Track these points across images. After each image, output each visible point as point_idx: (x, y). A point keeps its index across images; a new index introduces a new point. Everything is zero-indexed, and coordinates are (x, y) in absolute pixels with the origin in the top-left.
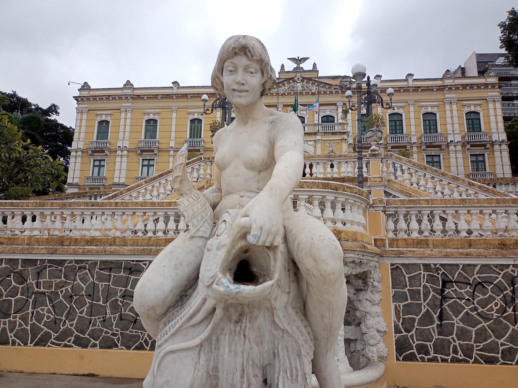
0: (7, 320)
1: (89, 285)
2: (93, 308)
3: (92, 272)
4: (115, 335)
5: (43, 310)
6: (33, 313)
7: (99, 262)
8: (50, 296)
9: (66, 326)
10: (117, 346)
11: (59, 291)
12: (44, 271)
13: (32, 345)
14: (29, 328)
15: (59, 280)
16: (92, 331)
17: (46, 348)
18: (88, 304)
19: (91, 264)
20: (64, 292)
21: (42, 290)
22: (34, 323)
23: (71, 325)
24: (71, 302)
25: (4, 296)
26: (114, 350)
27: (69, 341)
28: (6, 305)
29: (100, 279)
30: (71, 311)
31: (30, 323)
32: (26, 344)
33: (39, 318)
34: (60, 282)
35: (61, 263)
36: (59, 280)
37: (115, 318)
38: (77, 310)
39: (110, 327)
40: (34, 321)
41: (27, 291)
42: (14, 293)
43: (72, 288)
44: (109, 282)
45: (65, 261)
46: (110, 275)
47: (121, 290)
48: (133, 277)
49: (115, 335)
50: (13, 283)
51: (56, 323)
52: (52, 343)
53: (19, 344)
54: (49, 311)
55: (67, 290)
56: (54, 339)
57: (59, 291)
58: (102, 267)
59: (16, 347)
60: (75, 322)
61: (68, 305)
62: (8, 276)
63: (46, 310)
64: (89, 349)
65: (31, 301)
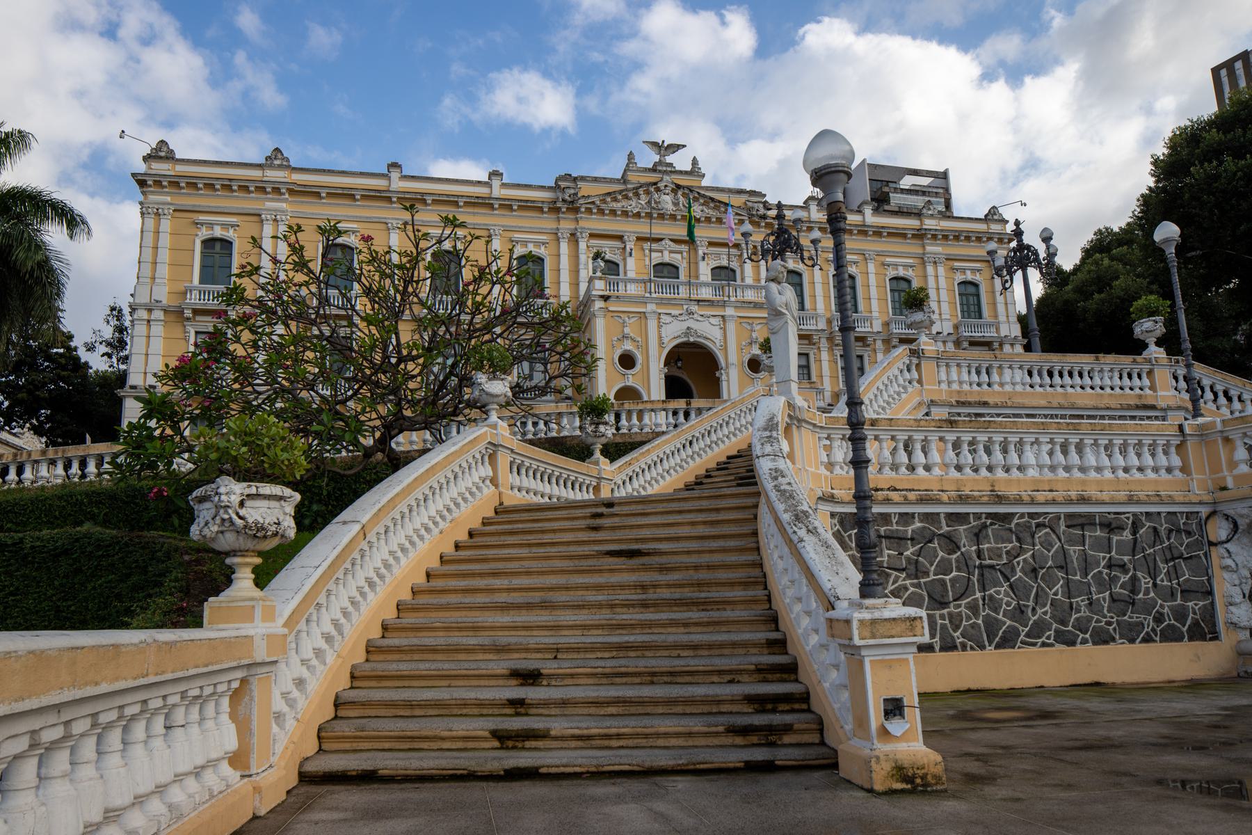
0: (945, 611)
1: (1056, 552)
4: (1109, 623)
5: (998, 593)
6: (984, 600)
10: (1113, 640)
13: (992, 647)
14: (980, 622)
16: (1077, 619)
17: (1016, 650)
21: (988, 562)
23: (1045, 612)
26: (1112, 646)
27: (1048, 638)
28: (939, 588)
29: (1072, 542)
32: (982, 647)
33: (994, 604)
34: (1013, 548)
35: (1007, 517)
37: (1104, 599)
39: (1099, 612)
41: (965, 563)
42: (944, 568)
45: (1013, 515)
46: (1083, 535)
47: (1104, 558)
48: (1115, 538)
49: (1109, 623)
51: (1022, 612)
54: (1007, 595)
58: (1069, 523)
60: (1048, 608)
62: (930, 541)
63: (1001, 591)
64: (1078, 646)
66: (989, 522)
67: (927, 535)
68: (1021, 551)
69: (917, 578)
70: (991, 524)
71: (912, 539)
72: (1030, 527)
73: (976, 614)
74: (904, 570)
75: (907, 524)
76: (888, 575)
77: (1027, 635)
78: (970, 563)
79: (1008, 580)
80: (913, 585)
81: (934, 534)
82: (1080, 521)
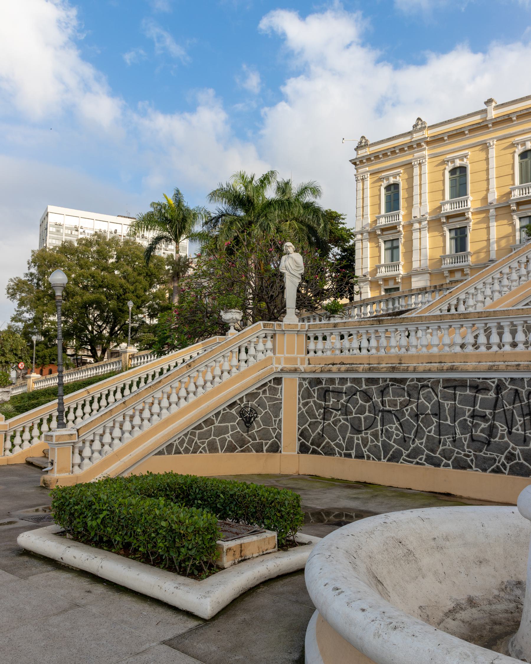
0: (359, 436)
1: (434, 404)
2: (441, 427)
3: (436, 391)
6: (382, 430)
7: (441, 380)
8: (396, 414)
9: (415, 444)
11: (404, 409)
12: (387, 390)
13: (385, 460)
14: (380, 444)
15: (403, 399)
17: (399, 464)
18: (435, 424)
19: (433, 382)
20: (409, 410)
21: (388, 408)
22: (384, 440)
24: (418, 421)
25: (354, 413)
29: (445, 398)
30: (419, 430)
31: (381, 439)
32: (379, 459)
34: (404, 401)
36: (403, 399)
38: (425, 429)
40: (384, 438)
41: (374, 408)
42: (361, 411)
43: (417, 407)
44: (455, 401)
46: (455, 394)
50: (360, 402)
51: (405, 441)
52: (404, 460)
53: (373, 459)
55: (412, 408)
56: (406, 456)
57: (404, 409)
58: (446, 385)
59: (371, 461)
61: (415, 424)
62: (355, 394)
63: (394, 427)
65: (379, 418)
66: (390, 383)
67: (354, 391)
68: (409, 403)
69: (346, 415)
70: (392, 385)
71: (345, 393)
72: (417, 387)
73: (378, 440)
74: (340, 410)
75: (343, 384)
76: (332, 413)
77: (408, 456)
78: (377, 408)
79: (399, 420)
80: (343, 419)
81: (358, 391)
82: (454, 384)
